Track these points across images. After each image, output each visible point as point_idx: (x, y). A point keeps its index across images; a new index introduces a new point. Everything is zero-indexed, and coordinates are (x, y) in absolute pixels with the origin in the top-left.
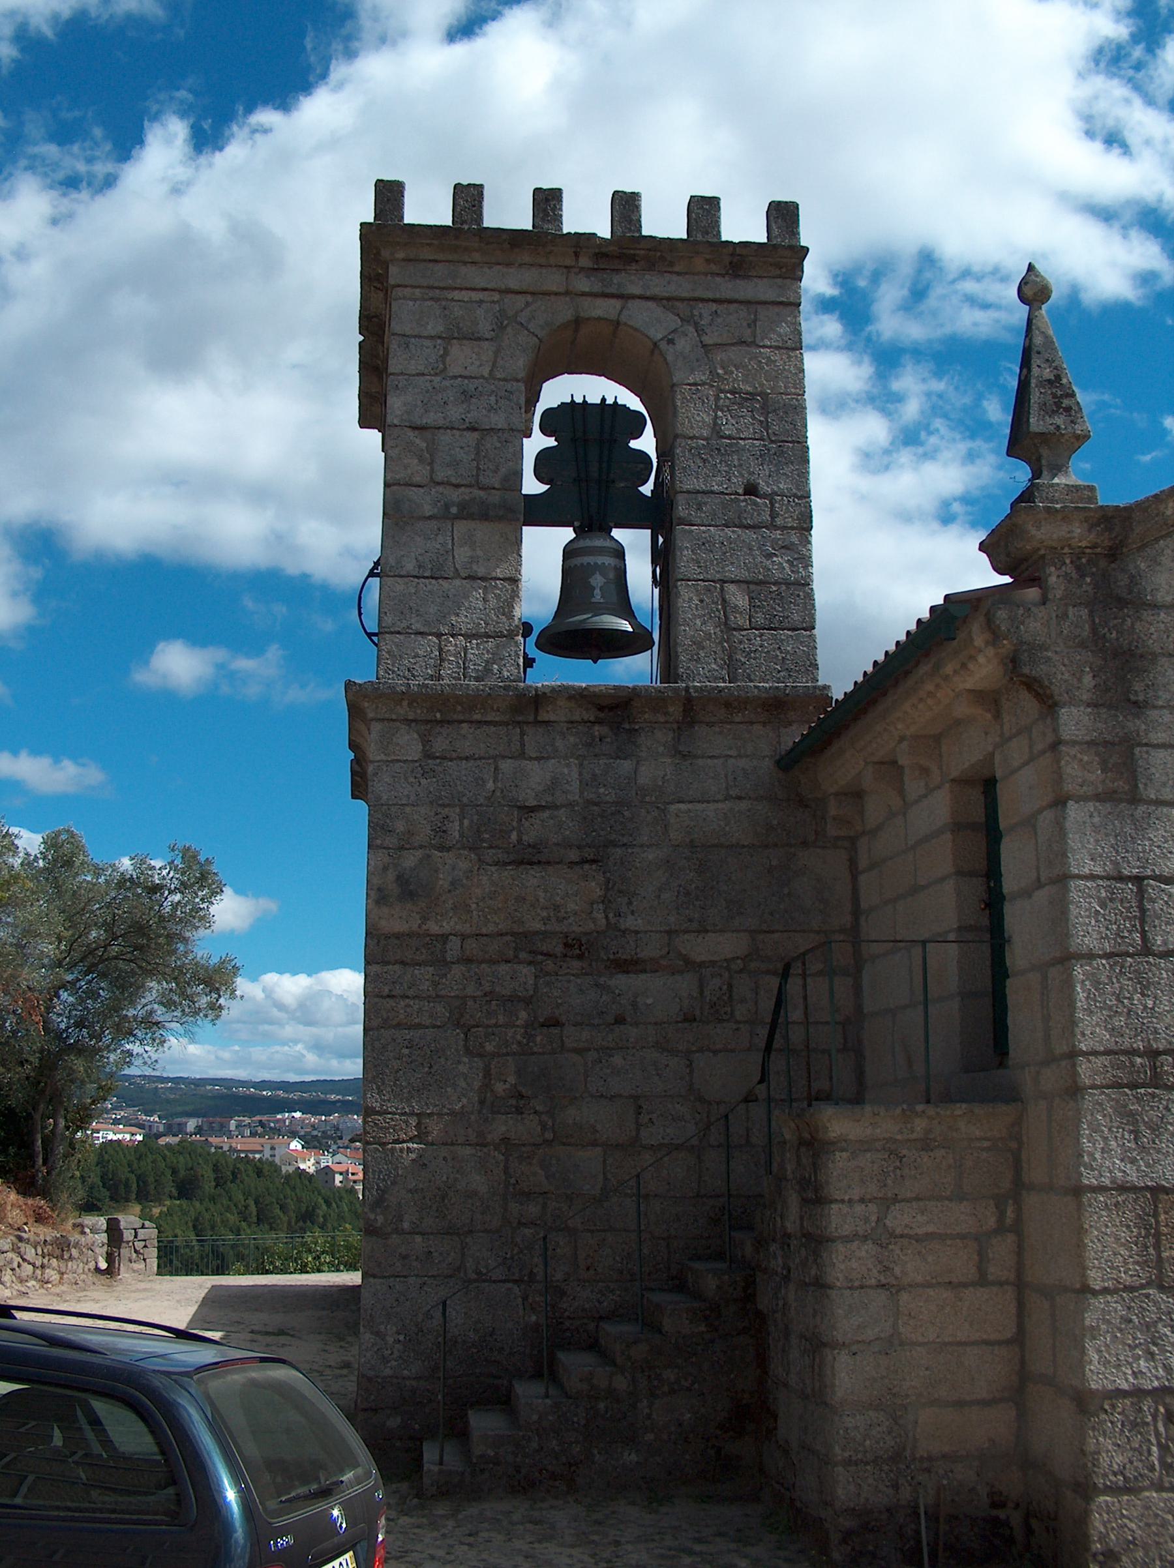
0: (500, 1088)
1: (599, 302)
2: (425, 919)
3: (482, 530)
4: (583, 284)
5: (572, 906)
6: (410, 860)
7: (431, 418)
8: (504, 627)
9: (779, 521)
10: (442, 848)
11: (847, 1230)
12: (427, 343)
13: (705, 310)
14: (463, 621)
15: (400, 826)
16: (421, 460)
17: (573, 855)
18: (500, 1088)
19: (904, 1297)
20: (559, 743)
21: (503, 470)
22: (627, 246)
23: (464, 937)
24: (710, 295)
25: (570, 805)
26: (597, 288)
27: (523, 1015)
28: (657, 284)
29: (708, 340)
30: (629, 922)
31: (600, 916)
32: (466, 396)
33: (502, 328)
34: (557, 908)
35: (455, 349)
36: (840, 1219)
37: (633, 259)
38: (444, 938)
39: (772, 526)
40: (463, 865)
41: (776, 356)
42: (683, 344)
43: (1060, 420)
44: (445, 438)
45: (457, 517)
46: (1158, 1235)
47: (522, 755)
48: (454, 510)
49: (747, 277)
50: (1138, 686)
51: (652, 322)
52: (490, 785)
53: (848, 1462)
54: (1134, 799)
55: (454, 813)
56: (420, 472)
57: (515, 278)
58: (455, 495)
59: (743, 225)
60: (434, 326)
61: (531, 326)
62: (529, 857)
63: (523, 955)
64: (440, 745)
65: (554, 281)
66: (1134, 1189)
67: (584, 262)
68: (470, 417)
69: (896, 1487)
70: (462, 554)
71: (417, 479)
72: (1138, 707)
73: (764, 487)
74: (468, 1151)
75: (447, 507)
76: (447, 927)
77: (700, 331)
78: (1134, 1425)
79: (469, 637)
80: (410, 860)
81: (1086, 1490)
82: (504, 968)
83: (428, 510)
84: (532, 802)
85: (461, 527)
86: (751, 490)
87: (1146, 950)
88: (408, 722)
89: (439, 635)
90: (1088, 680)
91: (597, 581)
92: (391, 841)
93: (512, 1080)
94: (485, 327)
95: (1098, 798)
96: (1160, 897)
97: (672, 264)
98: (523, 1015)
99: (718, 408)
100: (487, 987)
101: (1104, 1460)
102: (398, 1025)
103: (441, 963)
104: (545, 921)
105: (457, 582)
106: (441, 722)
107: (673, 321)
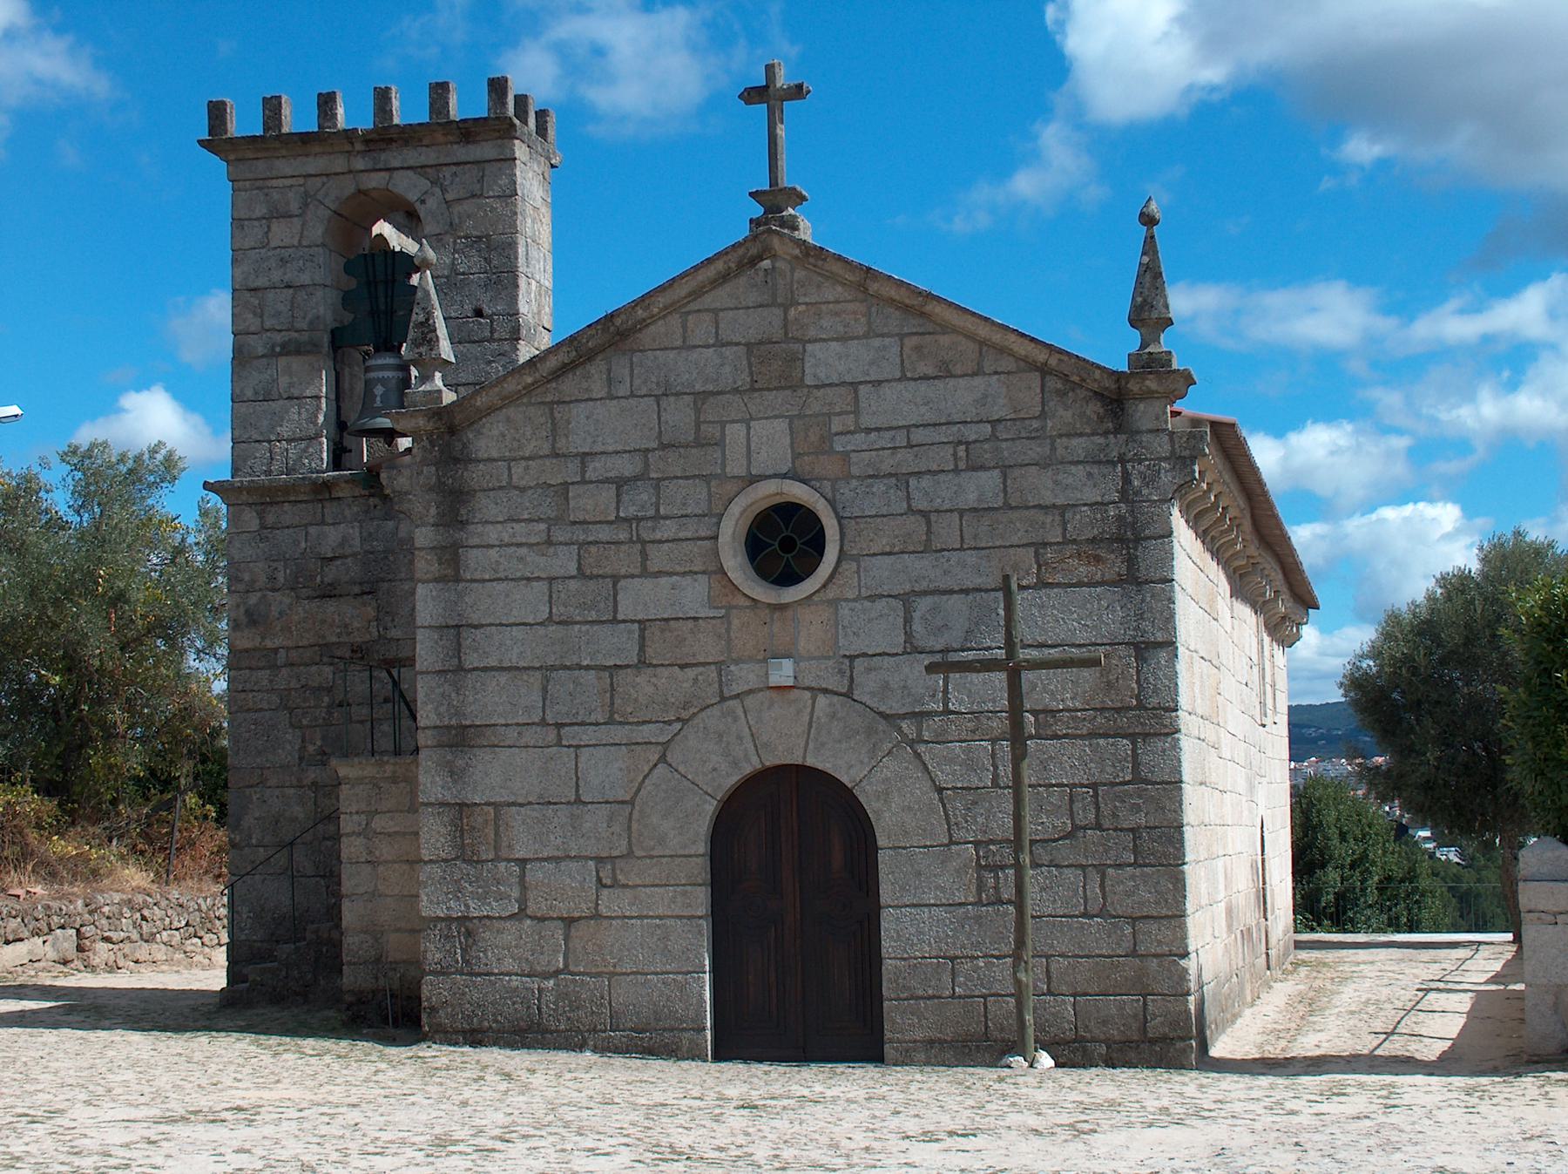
0: (311, 748)
1: (373, 175)
2: (263, 638)
3: (296, 363)
4: (359, 164)
5: (356, 624)
6: (253, 599)
7: (260, 283)
8: (312, 432)
9: (496, 336)
10: (274, 590)
11: (348, 830)
12: (256, 223)
13: (447, 172)
14: (285, 431)
15: (247, 577)
16: (255, 314)
17: (357, 589)
18: (311, 748)
19: (381, 868)
20: (347, 513)
21: (310, 316)
22: (385, 136)
23: (288, 649)
24: (448, 160)
25: (354, 555)
26: (370, 166)
27: (326, 699)
28: (413, 156)
29: (449, 197)
30: (394, 633)
31: (374, 631)
32: (283, 261)
33: (306, 205)
34: (346, 626)
35: (275, 226)
36: (347, 824)
37: (391, 140)
38: (276, 651)
39: (491, 340)
40: (287, 601)
41: (497, 204)
42: (432, 203)
43: (423, 350)
44: (271, 295)
45: (280, 354)
46: (462, 830)
47: (323, 523)
48: (278, 349)
49: (474, 142)
50: (463, 512)
51: (408, 186)
52: (303, 545)
53: (349, 963)
54: (457, 579)
55: (280, 565)
56: (253, 323)
57: (314, 165)
58: (278, 338)
59: (465, 104)
60: (261, 210)
61: (326, 202)
62: (328, 593)
63: (325, 659)
64: (270, 519)
65: (339, 164)
66: (448, 804)
67: (359, 146)
68: (286, 278)
69: (377, 978)
70: (283, 381)
71: (252, 329)
72: (463, 524)
73: (487, 311)
74: (292, 791)
75: (273, 347)
76: (277, 642)
77: (444, 190)
78: (447, 937)
79: (289, 441)
80: (253, 599)
81: (424, 973)
82: (314, 668)
83: (260, 351)
84: (330, 555)
85: (283, 361)
86: (479, 313)
87: (460, 669)
88: (250, 505)
89: (269, 442)
90: (433, 511)
91: (379, 390)
92: (241, 587)
93: (319, 743)
94: (294, 207)
95: (436, 580)
96: (468, 637)
97: (420, 140)
98: (326, 699)
99: (456, 251)
100: (303, 682)
101: (429, 955)
102: (249, 710)
103: (274, 667)
104: (339, 635)
105: (281, 402)
106: (271, 503)
107: (424, 184)
